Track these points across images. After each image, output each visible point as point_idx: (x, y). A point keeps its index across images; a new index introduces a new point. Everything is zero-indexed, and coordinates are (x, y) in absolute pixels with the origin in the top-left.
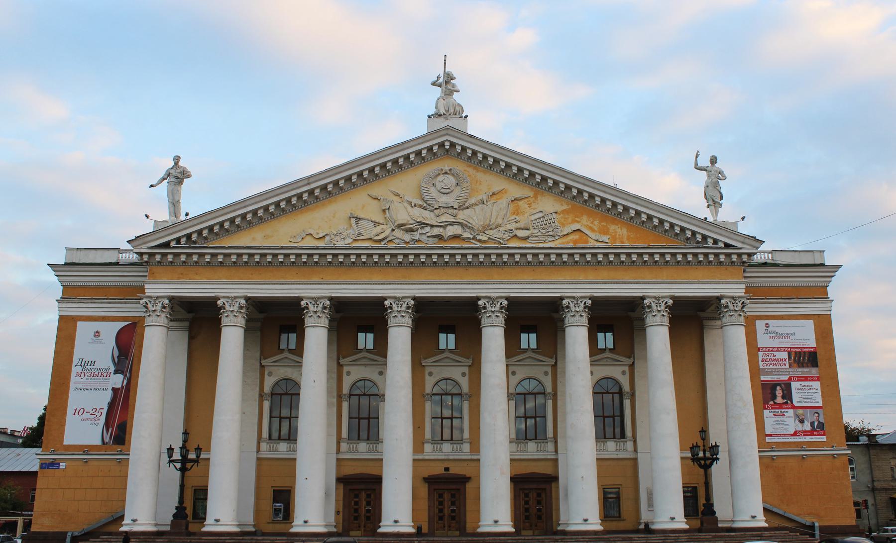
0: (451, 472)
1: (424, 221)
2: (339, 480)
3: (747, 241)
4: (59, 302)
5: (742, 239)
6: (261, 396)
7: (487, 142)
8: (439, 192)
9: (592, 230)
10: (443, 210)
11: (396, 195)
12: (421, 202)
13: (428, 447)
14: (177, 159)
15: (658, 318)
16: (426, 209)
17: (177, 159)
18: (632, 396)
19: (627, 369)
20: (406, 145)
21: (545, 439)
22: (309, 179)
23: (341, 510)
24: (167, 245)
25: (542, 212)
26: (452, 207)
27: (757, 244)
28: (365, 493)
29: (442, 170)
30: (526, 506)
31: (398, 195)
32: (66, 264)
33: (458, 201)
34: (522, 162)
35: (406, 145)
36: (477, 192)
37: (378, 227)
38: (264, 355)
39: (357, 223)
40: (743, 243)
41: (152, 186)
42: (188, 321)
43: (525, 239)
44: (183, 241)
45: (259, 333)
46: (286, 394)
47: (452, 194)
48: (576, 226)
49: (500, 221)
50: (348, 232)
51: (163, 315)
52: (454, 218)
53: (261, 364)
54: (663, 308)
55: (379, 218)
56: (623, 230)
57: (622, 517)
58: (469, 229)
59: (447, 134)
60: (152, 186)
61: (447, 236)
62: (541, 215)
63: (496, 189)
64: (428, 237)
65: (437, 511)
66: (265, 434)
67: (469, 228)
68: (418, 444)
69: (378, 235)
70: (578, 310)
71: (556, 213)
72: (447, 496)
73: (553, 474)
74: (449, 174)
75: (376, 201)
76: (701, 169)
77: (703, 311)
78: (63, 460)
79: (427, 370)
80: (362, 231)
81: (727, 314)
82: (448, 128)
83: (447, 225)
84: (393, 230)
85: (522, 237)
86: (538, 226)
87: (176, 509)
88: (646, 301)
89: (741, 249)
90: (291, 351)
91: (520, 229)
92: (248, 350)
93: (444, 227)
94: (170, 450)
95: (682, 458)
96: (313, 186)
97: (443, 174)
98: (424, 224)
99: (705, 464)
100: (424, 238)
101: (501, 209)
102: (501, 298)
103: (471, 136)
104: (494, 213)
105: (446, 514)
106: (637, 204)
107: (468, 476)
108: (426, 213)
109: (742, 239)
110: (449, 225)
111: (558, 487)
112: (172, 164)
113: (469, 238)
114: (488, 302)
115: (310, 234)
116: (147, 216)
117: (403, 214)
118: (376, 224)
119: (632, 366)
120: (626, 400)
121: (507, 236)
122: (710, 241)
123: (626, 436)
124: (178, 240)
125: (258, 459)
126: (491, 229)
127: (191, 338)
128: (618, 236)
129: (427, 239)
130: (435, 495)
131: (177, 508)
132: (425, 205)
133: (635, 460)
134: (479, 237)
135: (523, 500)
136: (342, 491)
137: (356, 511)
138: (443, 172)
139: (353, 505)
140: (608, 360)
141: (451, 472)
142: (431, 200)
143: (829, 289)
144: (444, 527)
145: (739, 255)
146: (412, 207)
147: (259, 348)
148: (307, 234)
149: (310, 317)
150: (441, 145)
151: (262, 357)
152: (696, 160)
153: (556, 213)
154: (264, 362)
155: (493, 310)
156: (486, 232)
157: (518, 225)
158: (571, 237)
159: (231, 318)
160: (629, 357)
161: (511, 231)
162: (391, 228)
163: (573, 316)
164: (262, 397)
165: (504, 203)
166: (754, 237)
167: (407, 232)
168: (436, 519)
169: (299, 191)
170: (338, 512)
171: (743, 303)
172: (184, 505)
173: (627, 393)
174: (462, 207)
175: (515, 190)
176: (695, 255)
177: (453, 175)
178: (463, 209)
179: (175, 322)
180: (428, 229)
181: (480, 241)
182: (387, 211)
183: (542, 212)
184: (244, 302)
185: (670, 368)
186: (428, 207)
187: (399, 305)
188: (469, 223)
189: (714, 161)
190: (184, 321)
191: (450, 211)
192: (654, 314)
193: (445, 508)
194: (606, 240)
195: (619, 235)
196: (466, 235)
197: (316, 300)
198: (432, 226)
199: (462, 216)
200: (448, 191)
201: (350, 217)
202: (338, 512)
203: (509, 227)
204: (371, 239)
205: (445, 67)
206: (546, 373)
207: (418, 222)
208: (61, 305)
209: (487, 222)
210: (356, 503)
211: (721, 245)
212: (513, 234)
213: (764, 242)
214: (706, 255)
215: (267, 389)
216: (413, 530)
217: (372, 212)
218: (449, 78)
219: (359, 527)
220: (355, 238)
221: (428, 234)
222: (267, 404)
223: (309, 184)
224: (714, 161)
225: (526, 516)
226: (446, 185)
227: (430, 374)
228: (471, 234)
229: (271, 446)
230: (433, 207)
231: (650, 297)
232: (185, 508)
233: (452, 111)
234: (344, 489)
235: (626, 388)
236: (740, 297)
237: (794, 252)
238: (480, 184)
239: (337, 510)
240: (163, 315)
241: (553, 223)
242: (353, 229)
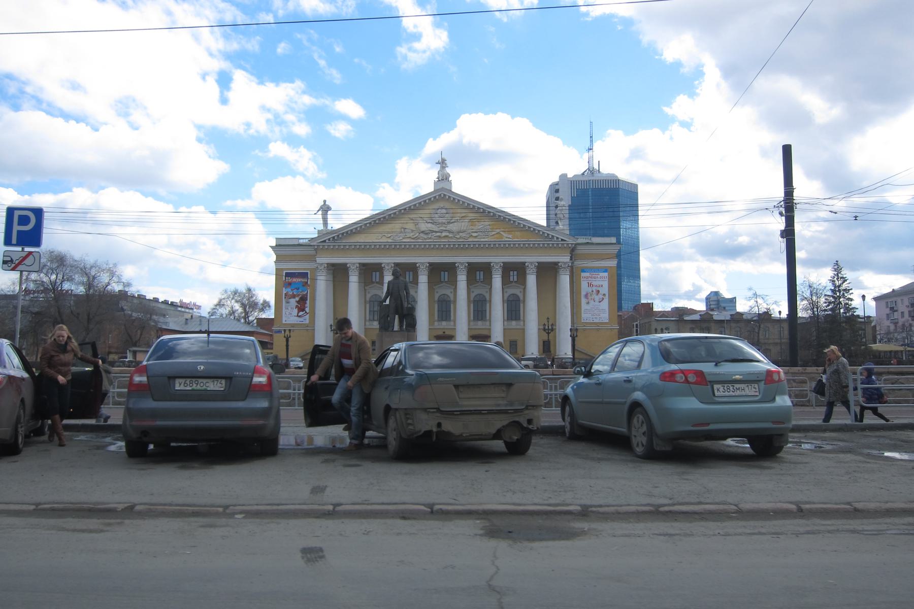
0: (446, 333)
10: (440, 225)
13: (436, 323)
14: (325, 201)
15: (531, 271)
17: (325, 201)
19: (522, 290)
21: (486, 320)
24: (325, 241)
38: (365, 285)
43: (476, 237)
44: (331, 240)
46: (376, 301)
48: (498, 231)
59: (443, 191)
62: (483, 226)
66: (368, 318)
68: (431, 322)
69: (413, 236)
73: (488, 334)
79: (436, 290)
82: (443, 188)
89: (568, 241)
90: (377, 282)
93: (441, 232)
94: (331, 326)
95: (539, 329)
99: (548, 332)
102: (465, 262)
108: (433, 226)
112: (323, 203)
116: (315, 228)
117: (424, 227)
119: (525, 289)
122: (555, 238)
124: (329, 239)
125: (365, 328)
127: (334, 277)
133: (524, 329)
134: (457, 236)
145: (568, 244)
154: (366, 288)
158: (496, 236)
174: (449, 223)
181: (456, 238)
184: (358, 265)
185: (535, 292)
191: (444, 225)
194: (511, 237)
196: (451, 235)
197: (388, 264)
198: (436, 232)
206: (487, 292)
207: (431, 231)
211: (560, 240)
214: (553, 244)
215: (368, 299)
217: (410, 226)
222: (368, 306)
227: (437, 292)
231: (528, 262)
233: (445, 177)
236: (567, 262)
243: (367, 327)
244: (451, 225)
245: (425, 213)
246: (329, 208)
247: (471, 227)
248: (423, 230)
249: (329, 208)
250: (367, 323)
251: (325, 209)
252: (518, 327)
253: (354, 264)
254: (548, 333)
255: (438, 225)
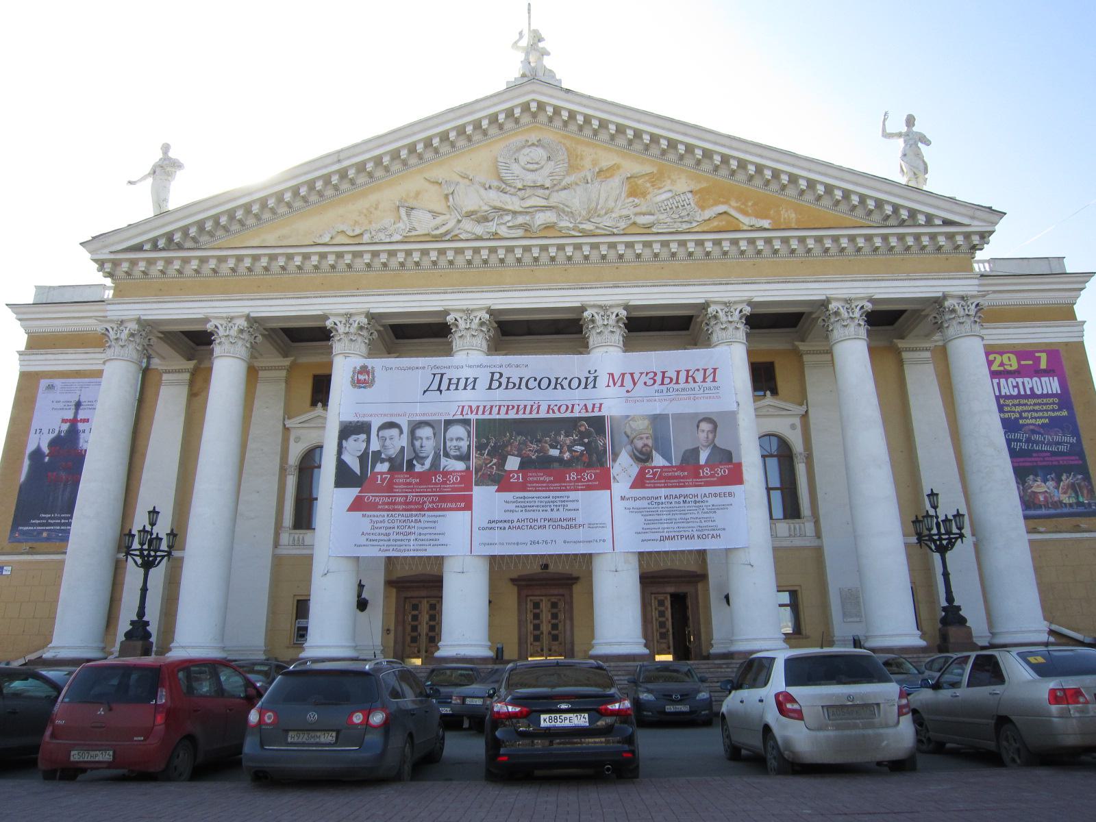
1: (503, 206)
2: (390, 583)
3: (978, 213)
4: (21, 353)
5: (970, 213)
6: (283, 470)
7: (590, 98)
8: (524, 169)
9: (745, 213)
10: (529, 192)
11: (464, 178)
12: (495, 183)
14: (166, 148)
15: (852, 329)
16: (506, 193)
17: (166, 148)
18: (807, 458)
19: (797, 421)
20: (478, 106)
22: (338, 155)
23: (392, 628)
24: (138, 248)
25: (670, 191)
26: (542, 187)
27: (993, 218)
28: (428, 602)
29: (527, 141)
30: (661, 619)
31: (465, 177)
32: (33, 304)
33: (551, 178)
34: (639, 121)
35: (478, 106)
36: (578, 169)
37: (438, 218)
39: (408, 215)
40: (973, 218)
41: (130, 182)
42: (188, 371)
45: (283, 385)
47: (542, 171)
48: (722, 208)
49: (611, 204)
50: (396, 226)
51: (131, 346)
52: (545, 201)
53: (284, 425)
54: (857, 314)
55: (439, 206)
56: (789, 212)
57: (804, 632)
58: (566, 216)
59: (533, 92)
60: (130, 182)
61: (536, 226)
62: (669, 195)
63: (605, 164)
64: (509, 227)
65: (531, 627)
67: (567, 214)
69: (437, 228)
70: (730, 319)
71: (691, 192)
72: (545, 606)
73: (699, 572)
74: (537, 146)
75: (436, 187)
76: (891, 136)
77: (902, 338)
78: (8, 563)
80: (416, 225)
81: (954, 322)
83: (536, 211)
84: (459, 221)
85: (644, 225)
86: (666, 209)
87: (131, 624)
88: (833, 306)
91: (644, 214)
92: (267, 408)
96: (345, 164)
97: (529, 146)
98: (504, 210)
100: (503, 231)
101: (612, 188)
103: (568, 91)
104: (603, 195)
105: (544, 633)
106: (809, 170)
107: (575, 574)
108: (506, 198)
109: (970, 213)
110: (536, 211)
111: (707, 590)
112: (160, 155)
113: (568, 228)
114: (598, 314)
115: (343, 232)
117: (471, 200)
118: (435, 214)
119: (805, 417)
120: (800, 465)
121: (622, 225)
122: (922, 219)
123: (802, 515)
124: (154, 242)
126: (598, 216)
128: (782, 220)
129: (509, 231)
130: (529, 603)
131: (133, 623)
132: (504, 186)
133: (818, 552)
134: (581, 226)
135: (656, 609)
136: (394, 600)
137: (414, 629)
138: (530, 143)
139: (410, 620)
140: (770, 409)
141: (552, 568)
142: (511, 178)
143: (1077, 308)
144: (542, 650)
145: (967, 236)
146: (486, 189)
147: (282, 405)
148: (338, 232)
149: (339, 340)
150: (526, 107)
151: (286, 416)
152: (884, 125)
153: (691, 192)
155: (606, 323)
156: (592, 220)
157: (638, 210)
159: (227, 346)
160: (801, 404)
161: (628, 217)
162: (456, 220)
163: (724, 329)
164: (286, 470)
165: (617, 181)
166: (990, 208)
167: (479, 222)
168: (530, 639)
169: (325, 171)
170: (388, 630)
171: (977, 305)
172: (145, 619)
173: (801, 454)
174: (556, 187)
175: (632, 167)
176: (901, 238)
177: (543, 147)
178: (557, 191)
179: (171, 375)
180: (508, 218)
182: (451, 198)
183: (670, 191)
185: (874, 400)
186: (508, 188)
187: (469, 321)
188: (567, 206)
189: (910, 121)
190: (182, 372)
191: (540, 192)
192: (845, 323)
193: (542, 622)
195: (785, 219)
198: (515, 213)
199: (557, 198)
200: (536, 166)
201: (399, 207)
202: (388, 630)
203: (625, 212)
204: (429, 234)
205: (529, 24)
207: (495, 208)
208: (22, 357)
209: (593, 205)
210: (415, 618)
211: (938, 222)
212: (631, 222)
213: (1005, 214)
216: (489, 653)
218: (537, 38)
219: (419, 652)
220: (408, 235)
221: (510, 224)
223: (339, 161)
224: (910, 121)
225: (661, 633)
226: (533, 159)
228: (571, 223)
229: (296, 538)
230: (515, 187)
231: (837, 300)
232: (147, 623)
234: (397, 598)
235: (797, 445)
237: (1021, 260)
238: (582, 159)
239: (386, 628)
240: (131, 346)
241: (688, 205)
242: (403, 221)
243: (282, 551)
244: (563, 194)
245: (478, 160)
246: (177, 165)
247: (631, 199)
248: (471, 208)
249: (177, 165)
250: (285, 538)
251: (165, 168)
252: (798, 542)
253: (231, 319)
254: (942, 550)
255: (521, 194)
